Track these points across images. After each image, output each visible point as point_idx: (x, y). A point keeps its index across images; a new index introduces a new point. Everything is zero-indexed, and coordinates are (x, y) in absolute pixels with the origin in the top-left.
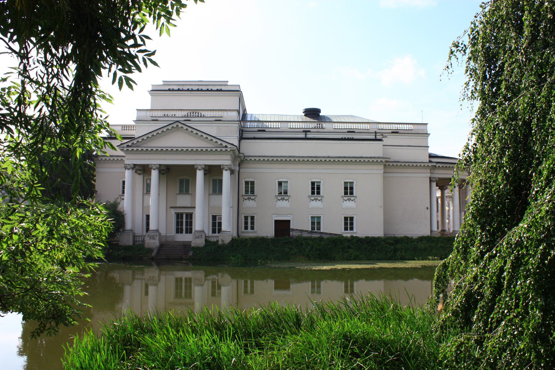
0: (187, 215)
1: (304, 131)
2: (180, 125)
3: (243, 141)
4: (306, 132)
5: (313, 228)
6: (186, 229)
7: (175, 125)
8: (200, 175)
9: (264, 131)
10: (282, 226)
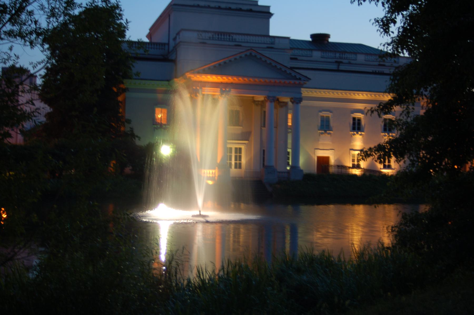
1: (336, 62)
4: (339, 63)
9: (296, 59)
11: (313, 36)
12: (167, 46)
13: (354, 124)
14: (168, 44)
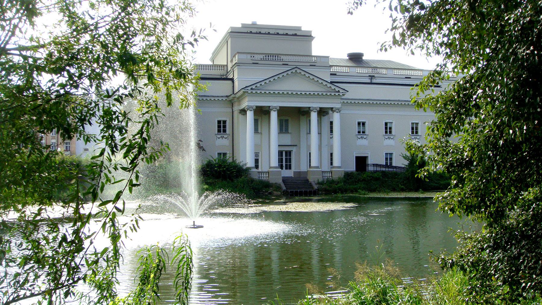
0: (286, 152)
1: (369, 76)
2: (299, 71)
4: (372, 77)
5: (386, 163)
6: (286, 165)
7: (294, 71)
8: (314, 116)
9: (335, 74)
10: (361, 161)
12: (225, 67)
14: (227, 65)
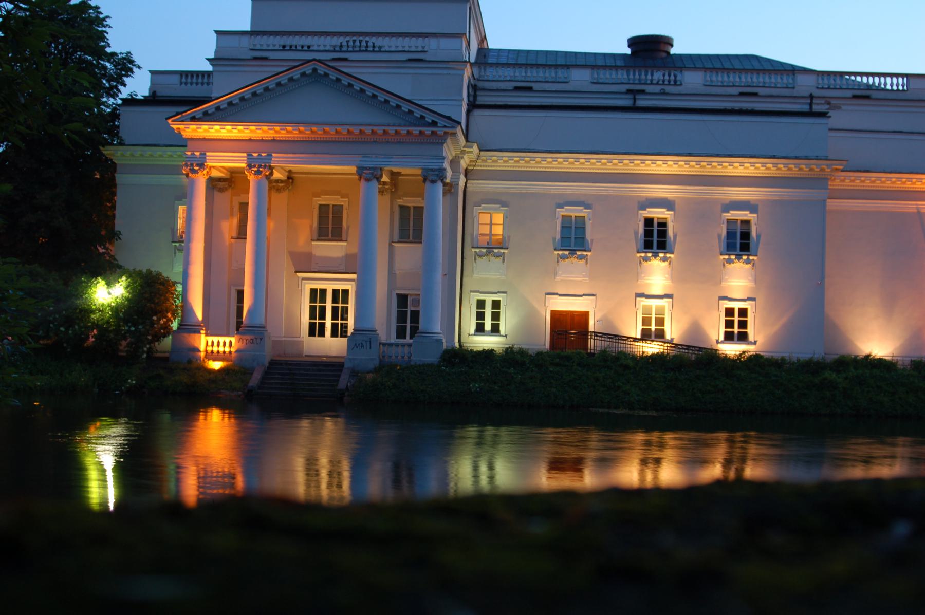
0: (335, 292)
1: (629, 92)
3: (477, 113)
9: (530, 89)
11: (634, 42)
13: (648, 233)
